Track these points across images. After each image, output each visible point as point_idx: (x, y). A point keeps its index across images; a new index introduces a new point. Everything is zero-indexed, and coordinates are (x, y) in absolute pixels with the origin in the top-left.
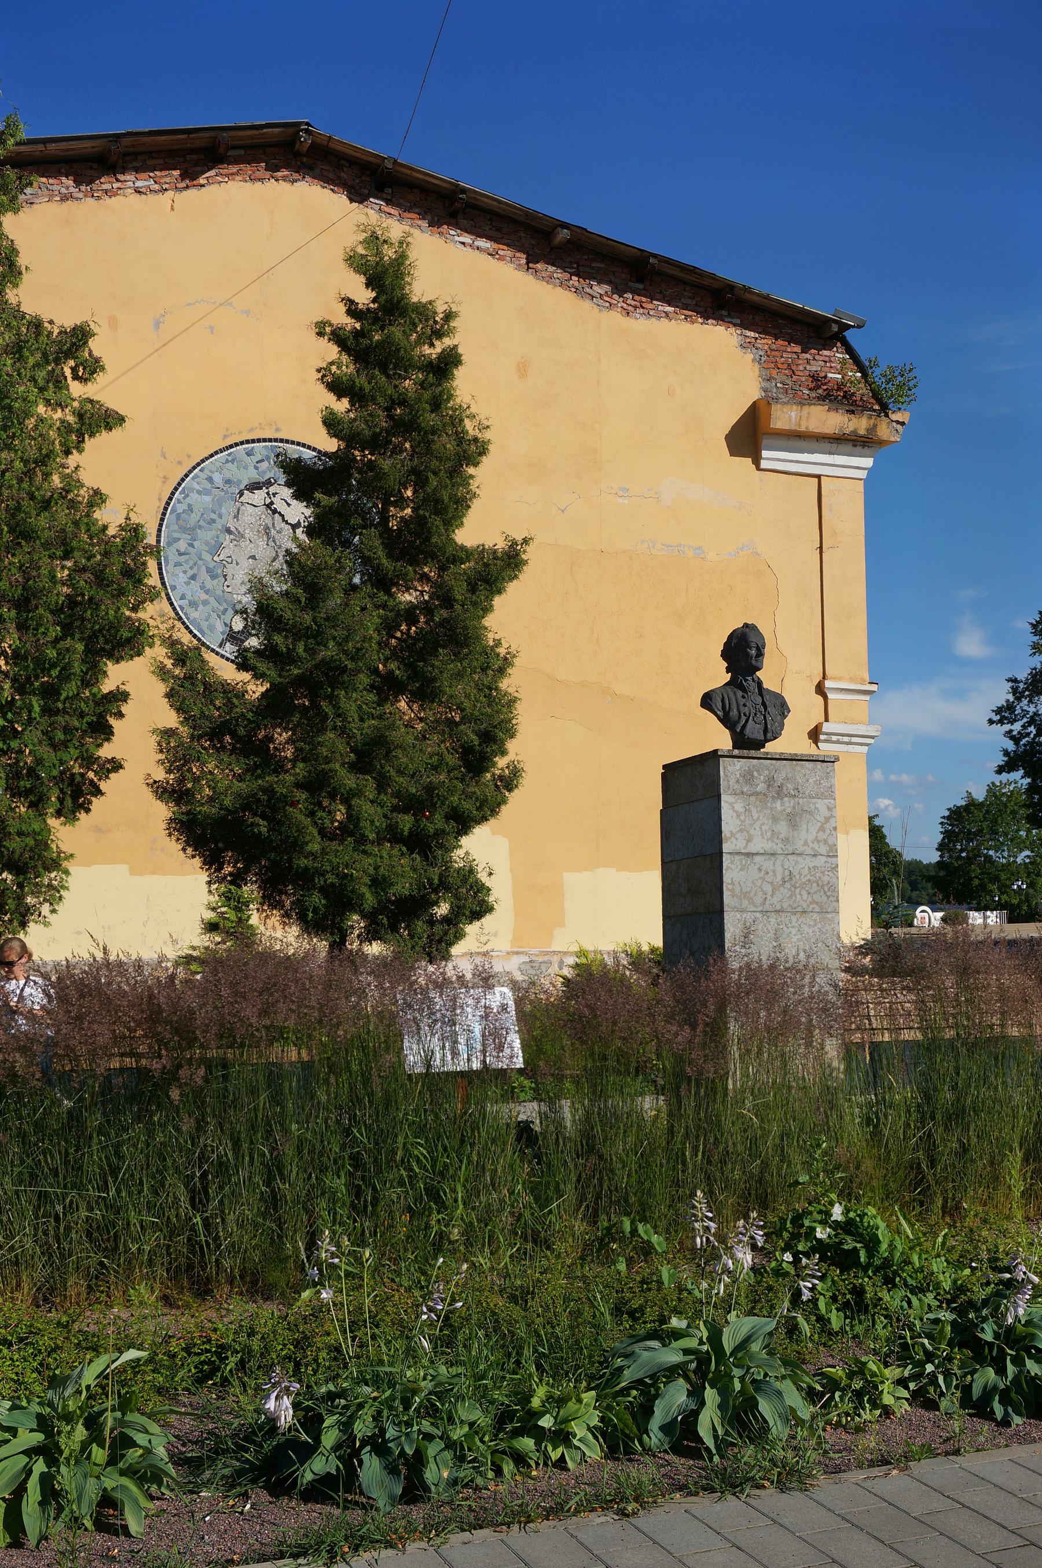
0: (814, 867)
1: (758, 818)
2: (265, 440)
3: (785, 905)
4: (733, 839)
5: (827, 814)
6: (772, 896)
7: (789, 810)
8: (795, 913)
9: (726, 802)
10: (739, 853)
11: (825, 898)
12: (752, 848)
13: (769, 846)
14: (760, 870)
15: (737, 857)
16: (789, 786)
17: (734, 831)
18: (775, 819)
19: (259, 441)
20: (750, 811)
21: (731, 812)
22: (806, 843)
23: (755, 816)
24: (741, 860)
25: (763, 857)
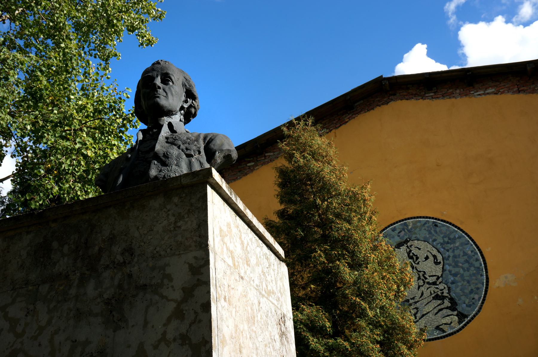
1: (49, 323)
2: (400, 221)
19: (397, 222)
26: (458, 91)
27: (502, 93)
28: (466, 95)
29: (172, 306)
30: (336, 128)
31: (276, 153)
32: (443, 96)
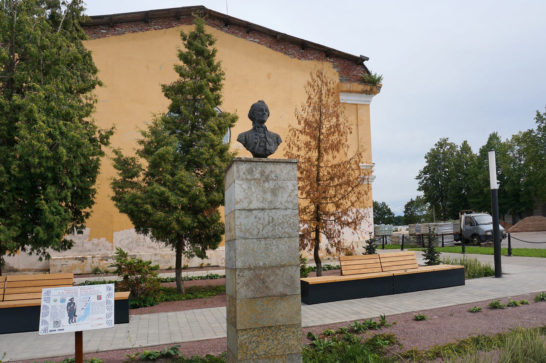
0: (285, 215)
1: (255, 192)
3: (270, 235)
4: (241, 203)
5: (293, 188)
6: (262, 230)
7: (272, 187)
8: (275, 239)
9: (238, 184)
10: (244, 210)
11: (291, 230)
12: (252, 206)
13: (261, 206)
14: (256, 217)
15: (243, 212)
16: (272, 175)
17: (242, 198)
18: (265, 192)
20: (250, 188)
21: (240, 189)
22: (281, 203)
23: (254, 190)
24: (245, 213)
25: (258, 211)
26: (240, 33)
27: (262, 44)
28: (244, 38)
29: (288, 194)
30: (167, 28)
31: (123, 30)
32: (233, 33)
